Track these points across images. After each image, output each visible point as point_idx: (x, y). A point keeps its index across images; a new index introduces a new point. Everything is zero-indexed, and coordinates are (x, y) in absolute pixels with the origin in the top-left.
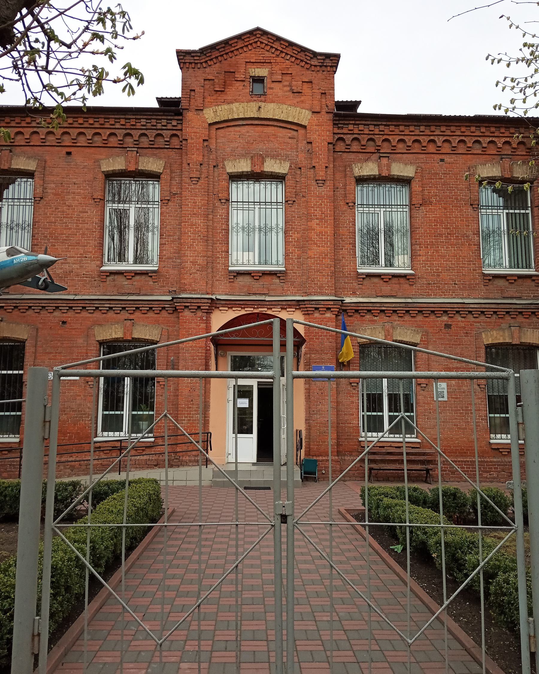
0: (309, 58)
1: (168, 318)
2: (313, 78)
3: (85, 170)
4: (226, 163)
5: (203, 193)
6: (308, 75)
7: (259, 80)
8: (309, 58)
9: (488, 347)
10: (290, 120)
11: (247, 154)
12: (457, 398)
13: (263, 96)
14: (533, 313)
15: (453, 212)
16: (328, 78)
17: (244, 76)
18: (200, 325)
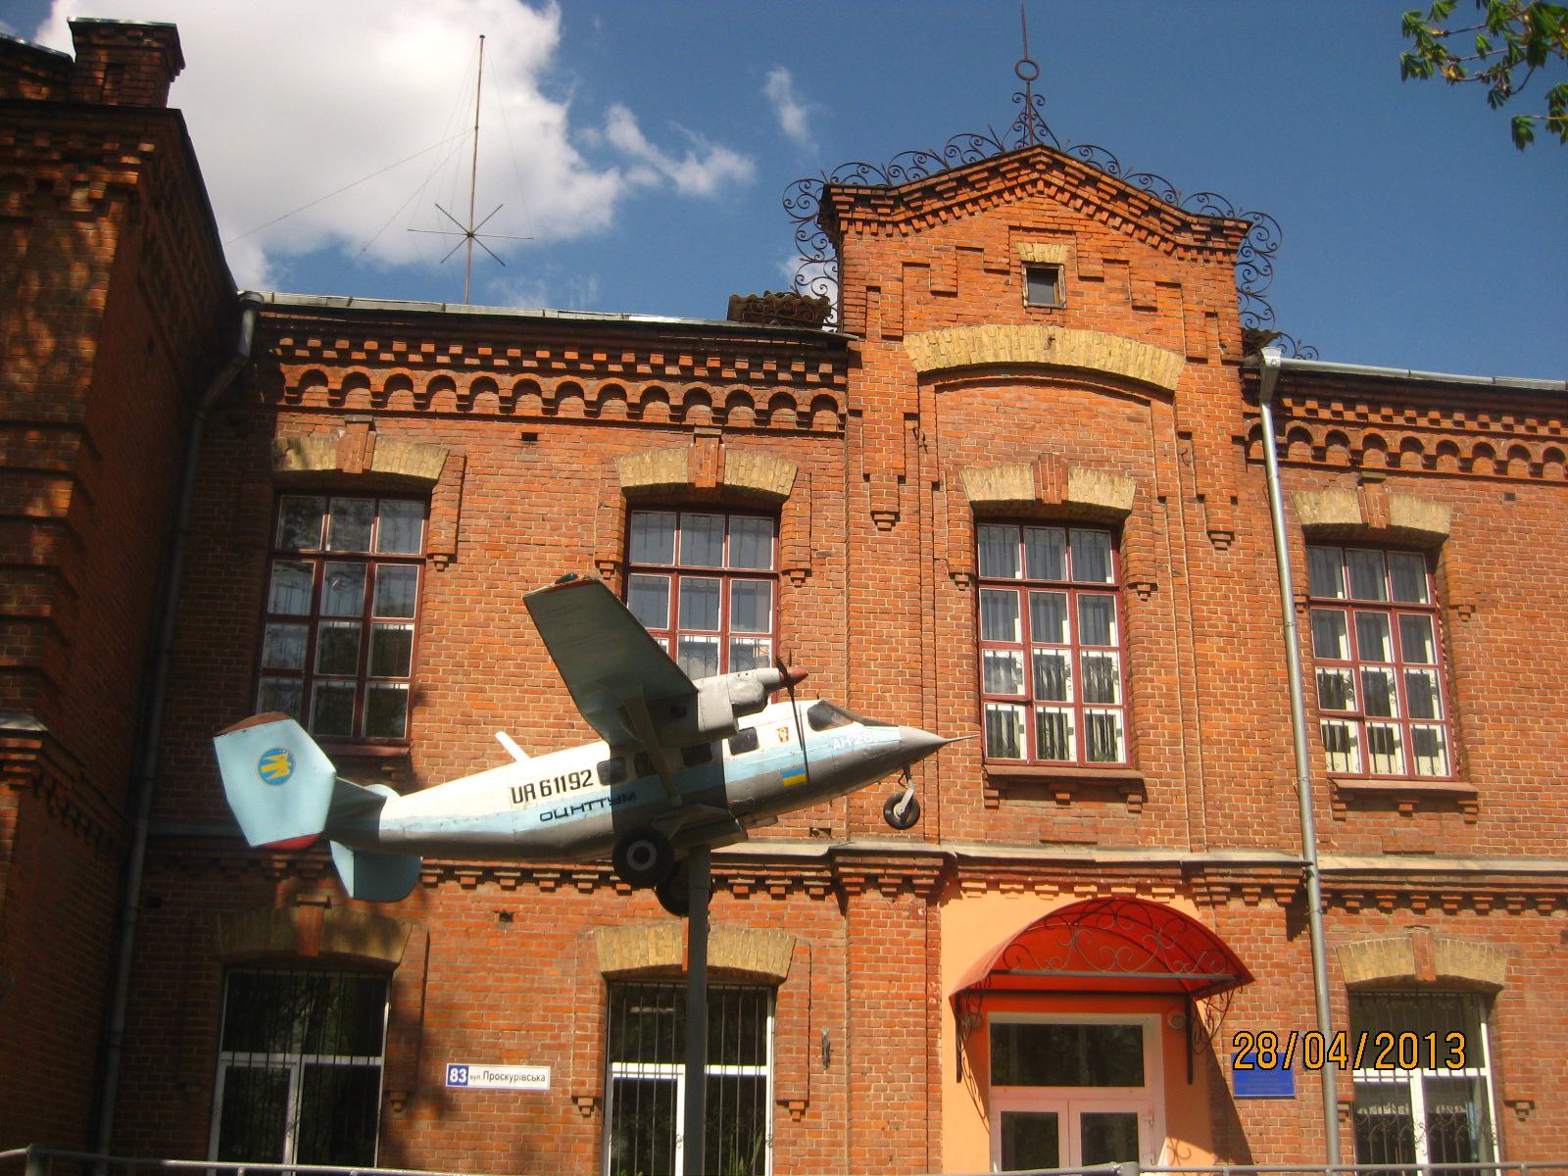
0: (1171, 229)
1: (810, 908)
2: (1184, 275)
3: (575, 482)
4: (966, 476)
5: (907, 555)
6: (1170, 269)
7: (1043, 274)
8: (1171, 229)
10: (1131, 374)
11: (1019, 454)
13: (1054, 312)
15: (1550, 630)
16: (1220, 278)
17: (1007, 260)
18: (909, 933)
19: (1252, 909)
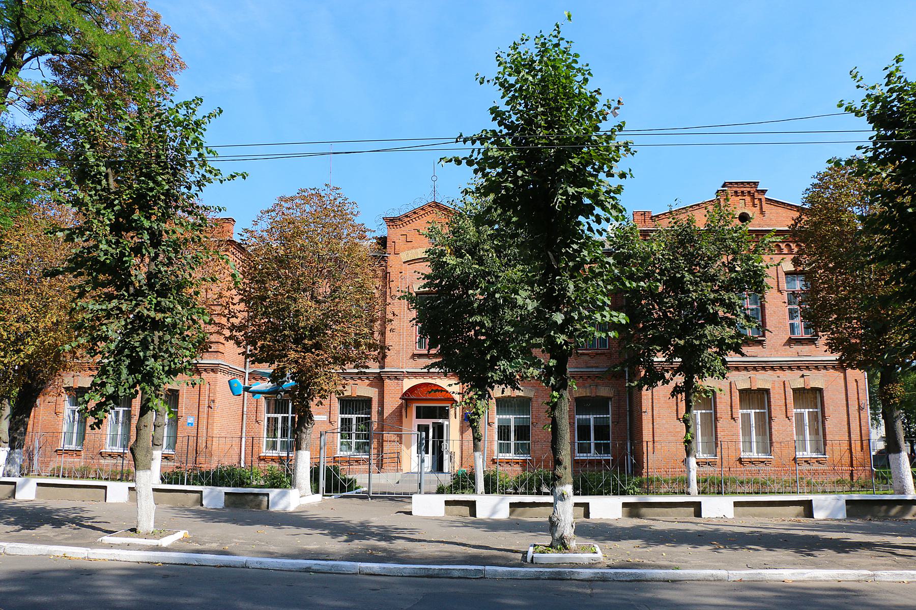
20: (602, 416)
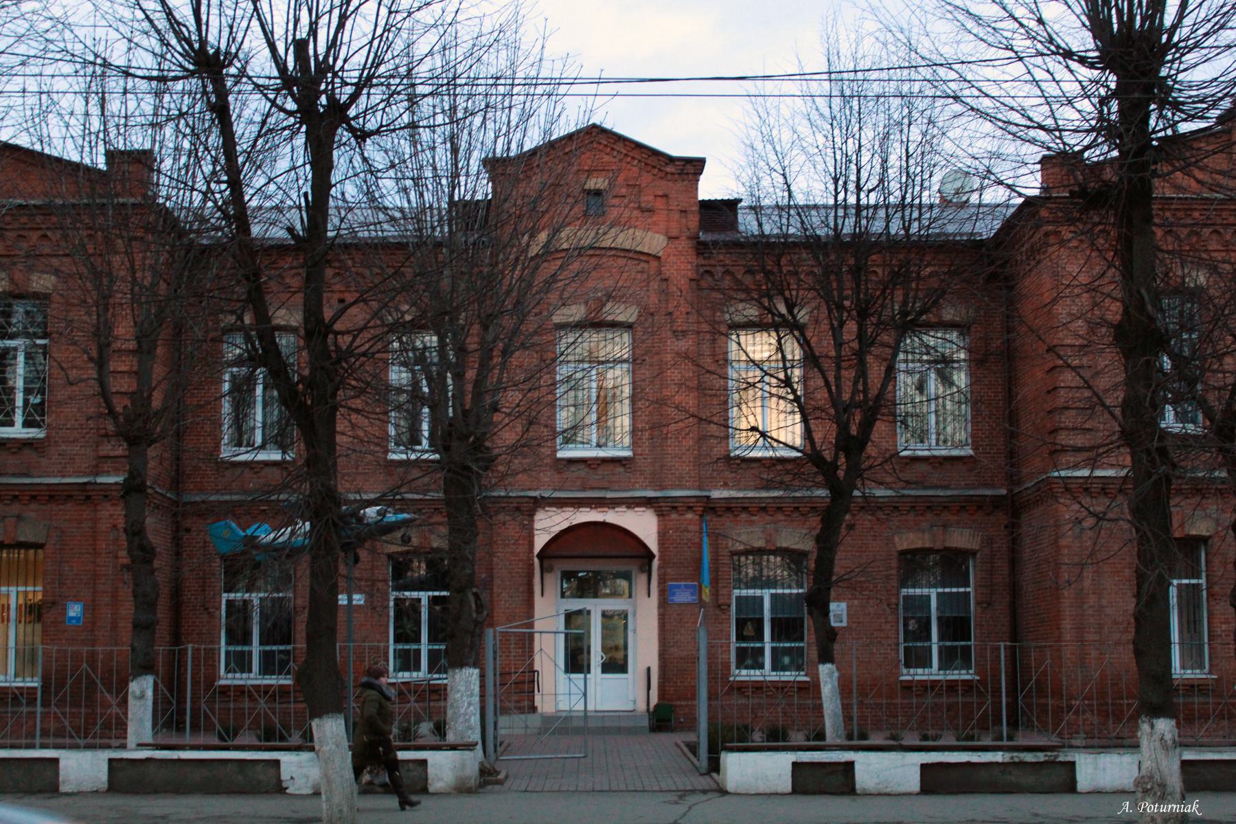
6: (663, 186)
7: (598, 193)
9: (903, 553)
12: (859, 623)
14: (962, 507)
19: (682, 518)
20: (954, 590)
